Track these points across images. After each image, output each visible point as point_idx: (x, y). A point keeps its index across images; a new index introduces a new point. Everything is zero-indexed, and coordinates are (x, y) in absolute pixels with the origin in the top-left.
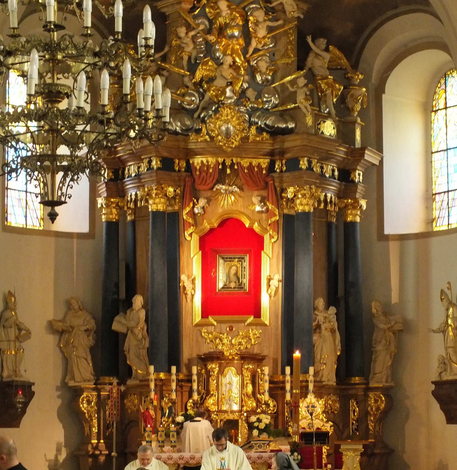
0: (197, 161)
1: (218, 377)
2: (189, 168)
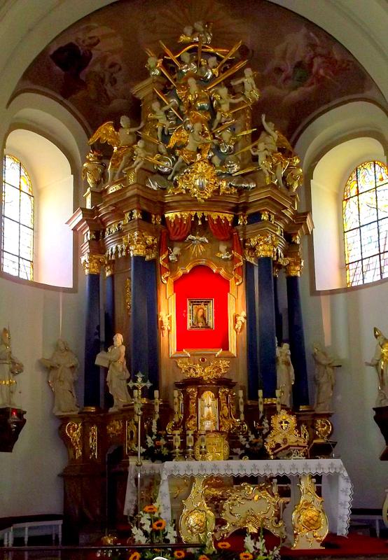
0: (170, 215)
1: (197, 401)
2: (164, 221)
